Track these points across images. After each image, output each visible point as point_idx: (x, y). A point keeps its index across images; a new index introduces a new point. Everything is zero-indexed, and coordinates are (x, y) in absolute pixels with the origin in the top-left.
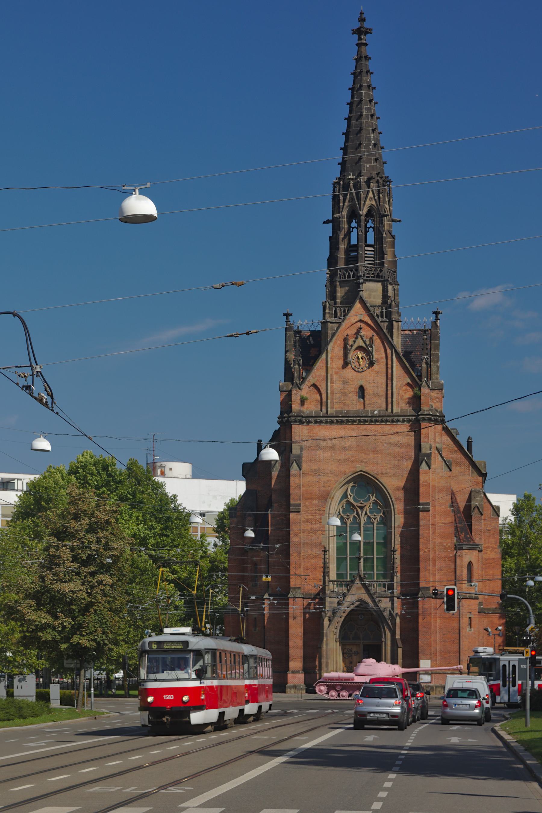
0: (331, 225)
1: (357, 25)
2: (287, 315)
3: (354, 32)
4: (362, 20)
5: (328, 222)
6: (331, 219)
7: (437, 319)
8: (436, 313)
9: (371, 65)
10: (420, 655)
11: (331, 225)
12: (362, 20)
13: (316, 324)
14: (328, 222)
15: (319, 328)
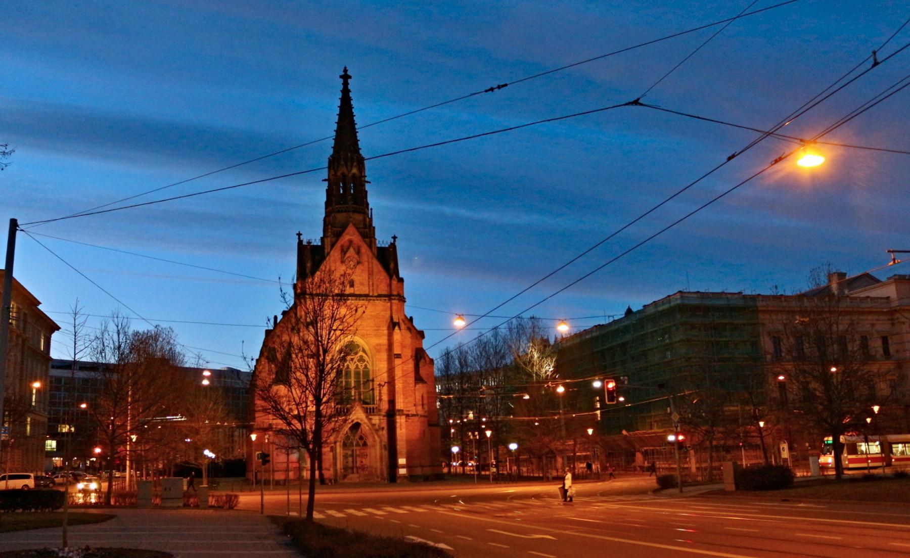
0: (327, 183)
1: (342, 73)
2: (299, 235)
3: (341, 77)
4: (345, 70)
5: (325, 180)
6: (327, 178)
7: (395, 241)
8: (395, 238)
9: (351, 95)
10: (399, 456)
11: (327, 183)
12: (345, 70)
13: (317, 241)
14: (325, 180)
15: (320, 244)
